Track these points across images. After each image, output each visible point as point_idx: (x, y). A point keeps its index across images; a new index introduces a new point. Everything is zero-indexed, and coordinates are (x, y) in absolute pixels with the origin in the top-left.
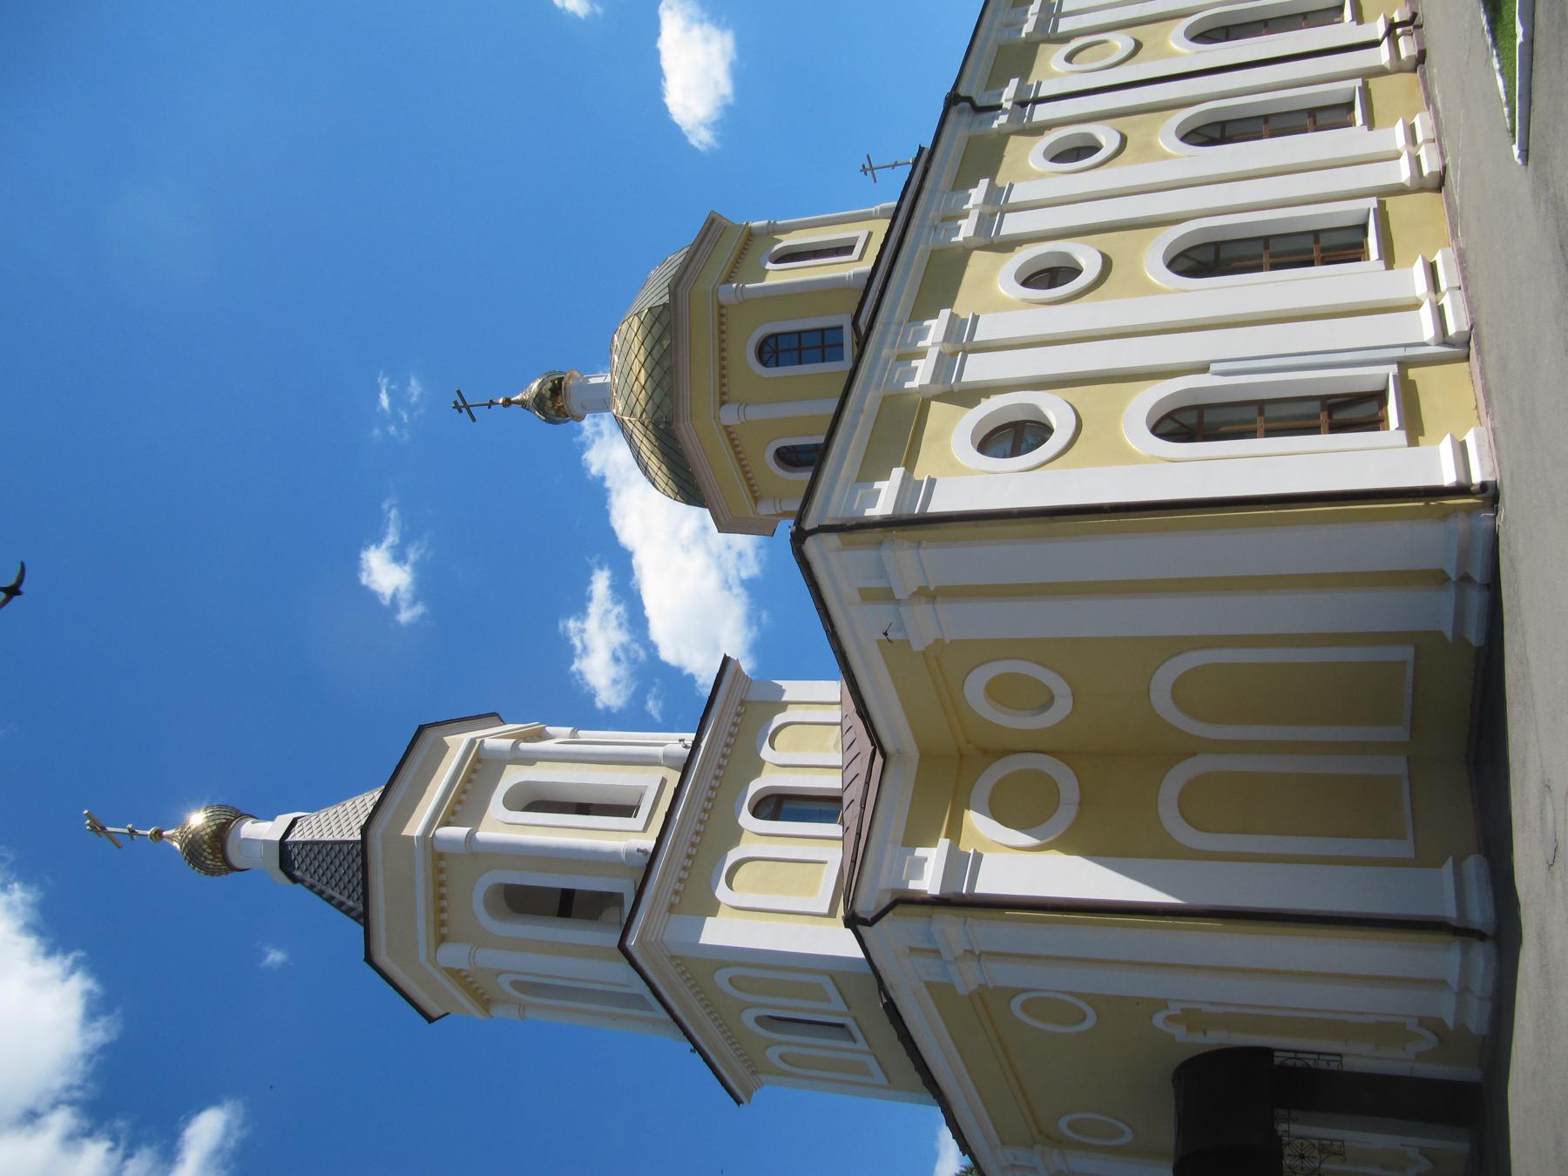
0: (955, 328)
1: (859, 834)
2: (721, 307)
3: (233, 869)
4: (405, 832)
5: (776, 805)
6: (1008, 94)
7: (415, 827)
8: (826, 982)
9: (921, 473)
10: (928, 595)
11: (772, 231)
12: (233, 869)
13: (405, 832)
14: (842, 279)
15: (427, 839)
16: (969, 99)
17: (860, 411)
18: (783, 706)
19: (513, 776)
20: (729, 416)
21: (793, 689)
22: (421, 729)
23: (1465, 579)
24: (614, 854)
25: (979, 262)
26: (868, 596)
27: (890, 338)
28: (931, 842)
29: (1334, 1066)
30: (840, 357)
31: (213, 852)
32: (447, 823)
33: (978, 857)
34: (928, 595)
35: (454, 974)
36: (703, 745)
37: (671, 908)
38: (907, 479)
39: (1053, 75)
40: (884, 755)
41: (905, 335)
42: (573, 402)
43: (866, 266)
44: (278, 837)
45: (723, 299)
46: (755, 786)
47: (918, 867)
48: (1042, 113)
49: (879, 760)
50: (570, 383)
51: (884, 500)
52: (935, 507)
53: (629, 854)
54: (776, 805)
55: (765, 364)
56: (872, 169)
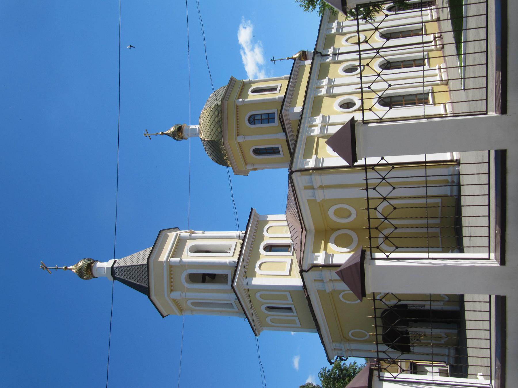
1: (301, 251)
2: (237, 106)
4: (160, 260)
5: (269, 248)
6: (330, 51)
7: (163, 257)
8: (288, 294)
9: (320, 156)
10: (322, 187)
11: (251, 82)
13: (160, 260)
14: (274, 99)
15: (167, 262)
16: (320, 53)
19: (190, 244)
20: (240, 139)
21: (270, 217)
22: (161, 231)
24: (225, 263)
25: (326, 101)
26: (306, 188)
27: (307, 121)
29: (423, 308)
30: (274, 122)
31: (87, 271)
32: (172, 257)
33: (333, 255)
34: (322, 187)
35: (174, 300)
38: (317, 158)
39: (343, 46)
40: (306, 230)
42: (185, 135)
43: (282, 95)
44: (111, 266)
45: (238, 104)
47: (316, 258)
48: (341, 57)
49: (304, 232)
50: (185, 127)
51: (311, 163)
52: (325, 165)
53: (230, 263)
54: (269, 248)
55: (250, 124)
56: (274, 60)
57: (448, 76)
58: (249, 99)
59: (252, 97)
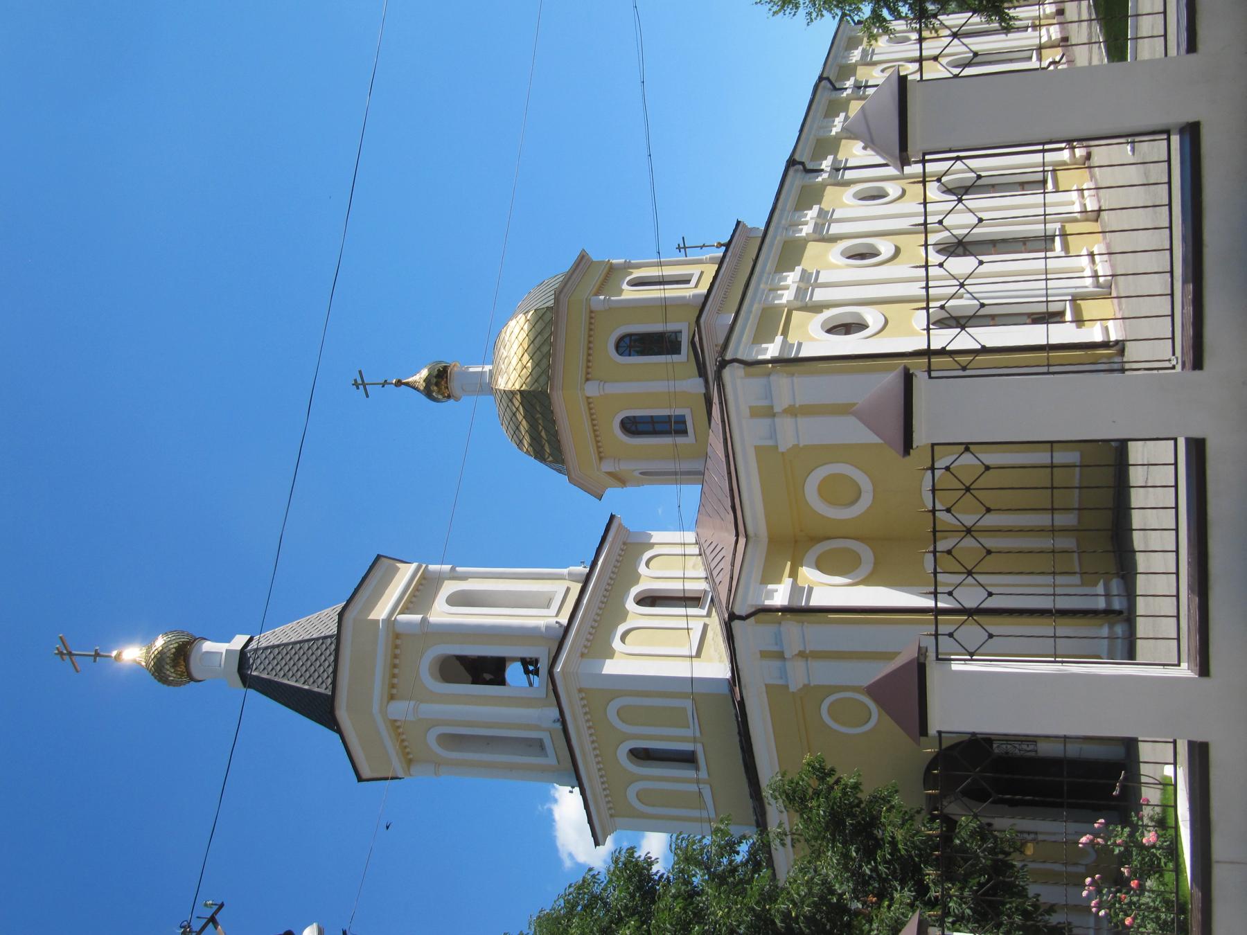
0: (805, 276)
1: (732, 578)
2: (592, 312)
3: (192, 679)
4: (372, 616)
5: (650, 600)
6: (826, 164)
7: (381, 612)
8: (688, 704)
9: (793, 338)
10: (792, 411)
11: (628, 267)
12: (192, 679)
13: (372, 616)
14: (684, 298)
15: (389, 621)
16: (802, 163)
17: (750, 312)
18: (651, 546)
19: (449, 588)
20: (592, 389)
21: (657, 537)
22: (379, 557)
23: (1133, 142)
24: (535, 629)
25: (813, 249)
26: (756, 413)
27: (764, 279)
28: (778, 580)
29: (1033, 754)
30: (679, 353)
31: (176, 664)
32: (402, 613)
33: (810, 589)
34: (792, 411)
35: (395, 725)
36: (600, 563)
37: (582, 655)
38: (785, 342)
39: (855, 156)
40: (747, 536)
41: (773, 280)
42: (455, 385)
43: (703, 289)
44: (239, 648)
45: (594, 307)
46: (634, 591)
47: (770, 595)
48: (849, 175)
49: (742, 541)
50: (456, 368)
51: (772, 350)
52: (803, 354)
53: (548, 628)
54: (650, 600)
55: (621, 354)
56: (685, 248)
57: (1099, 201)
58: (625, 296)
59: (629, 293)
